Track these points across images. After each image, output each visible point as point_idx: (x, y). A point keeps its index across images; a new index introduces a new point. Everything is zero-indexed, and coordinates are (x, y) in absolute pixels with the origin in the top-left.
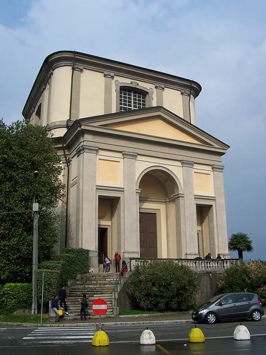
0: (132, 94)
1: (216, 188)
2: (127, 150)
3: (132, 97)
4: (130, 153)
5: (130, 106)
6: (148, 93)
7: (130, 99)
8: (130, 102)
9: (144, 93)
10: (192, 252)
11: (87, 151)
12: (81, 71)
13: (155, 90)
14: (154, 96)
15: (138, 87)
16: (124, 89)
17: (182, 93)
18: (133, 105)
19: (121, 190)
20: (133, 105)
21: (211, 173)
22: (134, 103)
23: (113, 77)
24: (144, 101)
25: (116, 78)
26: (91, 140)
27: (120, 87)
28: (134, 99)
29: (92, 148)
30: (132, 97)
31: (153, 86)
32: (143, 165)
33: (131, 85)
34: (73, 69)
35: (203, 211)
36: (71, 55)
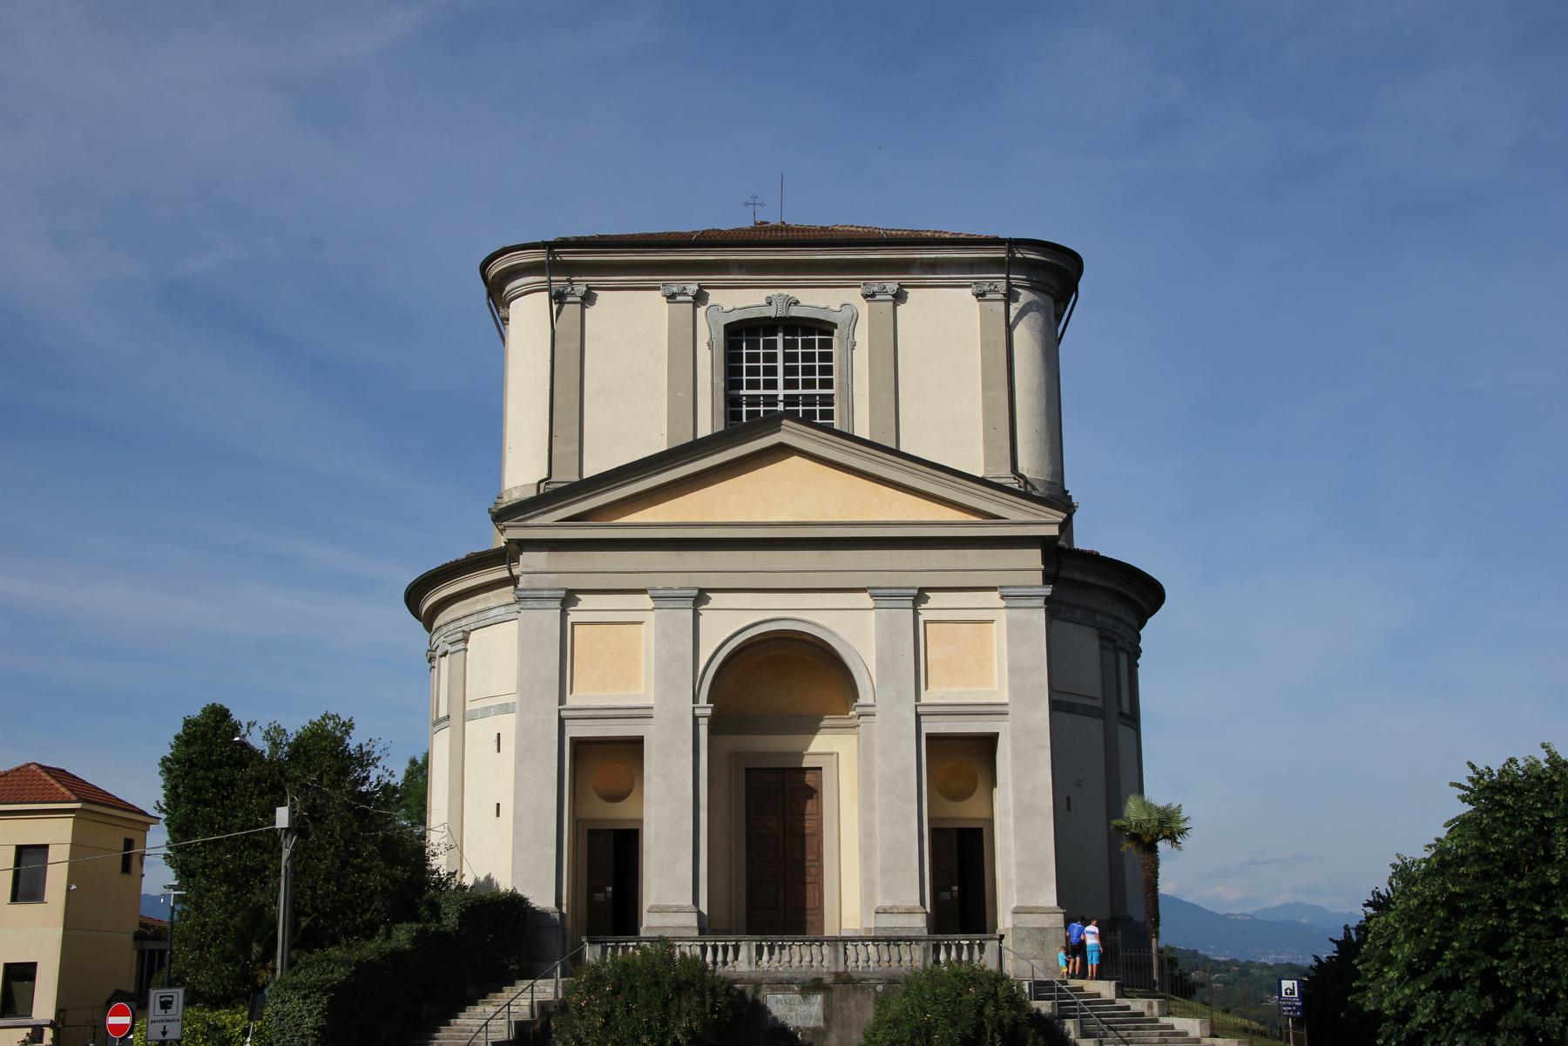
0: (780, 338)
1: (1015, 670)
2: (659, 582)
3: (780, 351)
4: (670, 593)
5: (772, 385)
6: (835, 326)
7: (773, 357)
8: (773, 371)
9: (821, 328)
10: (898, 903)
11: (530, 604)
12: (588, 299)
13: (863, 308)
14: (862, 335)
15: (794, 312)
16: (740, 333)
17: (980, 296)
18: (780, 378)
19: (643, 714)
20: (780, 378)
21: (1002, 617)
22: (787, 371)
23: (700, 298)
24: (827, 357)
25: (715, 296)
26: (544, 567)
27: (726, 326)
28: (787, 357)
29: (545, 594)
30: (780, 351)
31: (853, 296)
32: (727, 623)
33: (771, 312)
34: (559, 298)
35: (959, 760)
36: (539, 256)
